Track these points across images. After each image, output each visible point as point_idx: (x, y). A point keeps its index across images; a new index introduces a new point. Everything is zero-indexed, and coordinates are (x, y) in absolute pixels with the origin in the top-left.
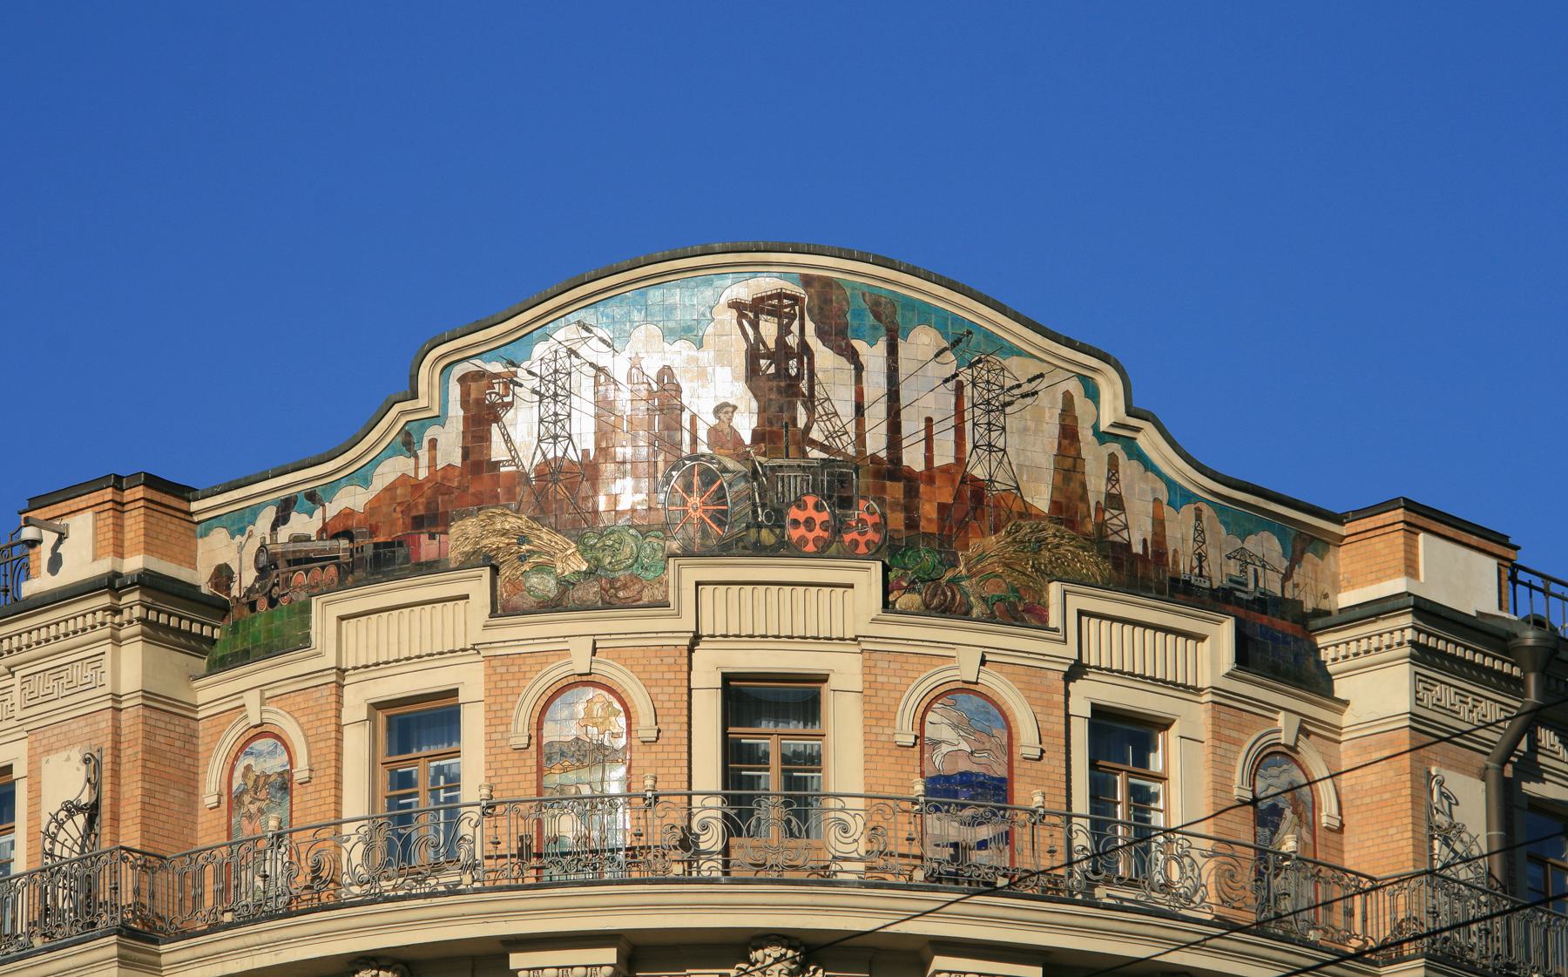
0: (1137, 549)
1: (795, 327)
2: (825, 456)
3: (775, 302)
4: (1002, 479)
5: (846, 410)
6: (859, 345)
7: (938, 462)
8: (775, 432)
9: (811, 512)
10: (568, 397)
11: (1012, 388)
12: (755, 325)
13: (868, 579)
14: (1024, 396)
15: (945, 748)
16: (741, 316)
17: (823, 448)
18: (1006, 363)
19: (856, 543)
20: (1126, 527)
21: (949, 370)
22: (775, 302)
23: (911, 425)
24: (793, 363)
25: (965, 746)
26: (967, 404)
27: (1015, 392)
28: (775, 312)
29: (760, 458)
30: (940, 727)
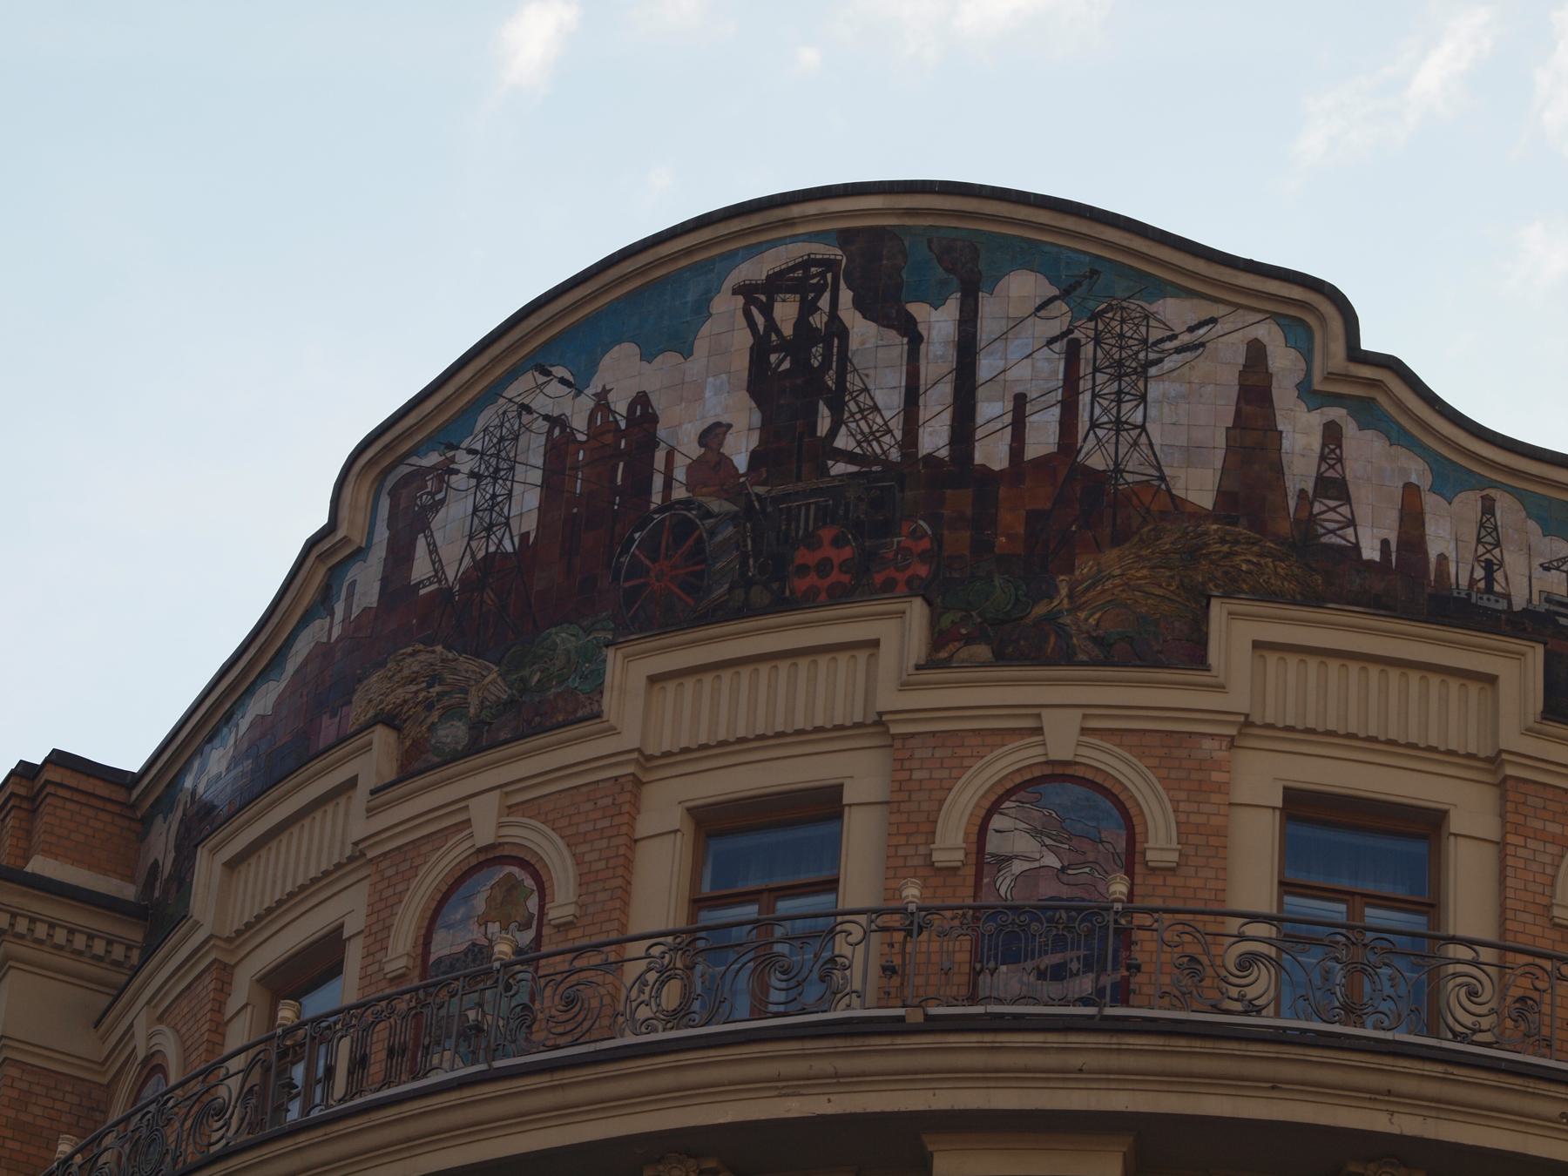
0: (1371, 552)
1: (824, 302)
2: (852, 469)
3: (799, 273)
4: (1136, 467)
5: (889, 400)
6: (918, 310)
7: (1032, 451)
9: (828, 551)
10: (512, 468)
11: (1162, 341)
12: (767, 311)
13: (903, 628)
14: (1178, 351)
15: (1018, 867)
18: (1152, 308)
20: (1352, 522)
21: (1056, 328)
22: (799, 273)
23: (991, 409)
24: (818, 350)
25: (1052, 861)
26: (1085, 368)
27: (1168, 345)
28: (798, 287)
29: (760, 490)
30: (1014, 837)
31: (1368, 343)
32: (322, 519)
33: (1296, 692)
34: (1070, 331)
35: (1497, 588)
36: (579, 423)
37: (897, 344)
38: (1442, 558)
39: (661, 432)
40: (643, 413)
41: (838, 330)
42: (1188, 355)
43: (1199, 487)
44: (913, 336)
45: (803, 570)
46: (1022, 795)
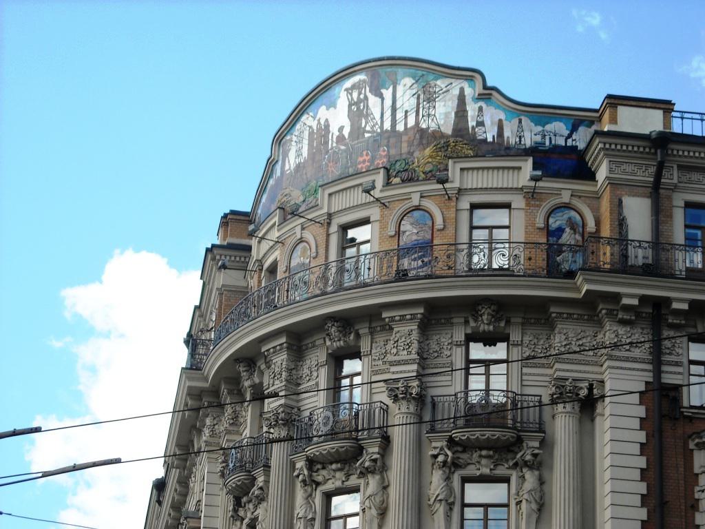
0: (490, 139)
2: (370, 135)
4: (433, 126)
5: (377, 116)
6: (383, 91)
8: (357, 131)
9: (365, 157)
12: (351, 95)
14: (443, 93)
16: (348, 92)
17: (369, 132)
19: (378, 164)
20: (485, 132)
21: (414, 91)
23: (400, 115)
24: (362, 104)
26: (421, 101)
27: (440, 92)
31: (490, 83)
32: (269, 154)
33: (473, 180)
34: (418, 92)
35: (522, 143)
36: (315, 128)
37: (379, 100)
38: (508, 137)
39: (331, 129)
40: (327, 126)
41: (366, 98)
42: (445, 94)
43: (448, 130)
44: (381, 96)
45: (360, 163)
46: (408, 215)
